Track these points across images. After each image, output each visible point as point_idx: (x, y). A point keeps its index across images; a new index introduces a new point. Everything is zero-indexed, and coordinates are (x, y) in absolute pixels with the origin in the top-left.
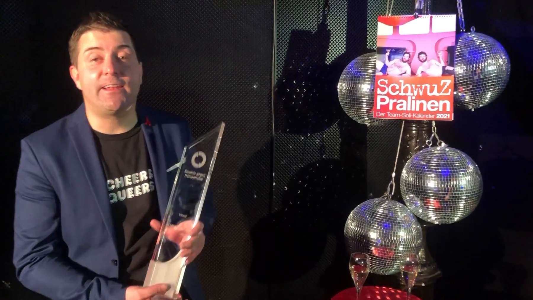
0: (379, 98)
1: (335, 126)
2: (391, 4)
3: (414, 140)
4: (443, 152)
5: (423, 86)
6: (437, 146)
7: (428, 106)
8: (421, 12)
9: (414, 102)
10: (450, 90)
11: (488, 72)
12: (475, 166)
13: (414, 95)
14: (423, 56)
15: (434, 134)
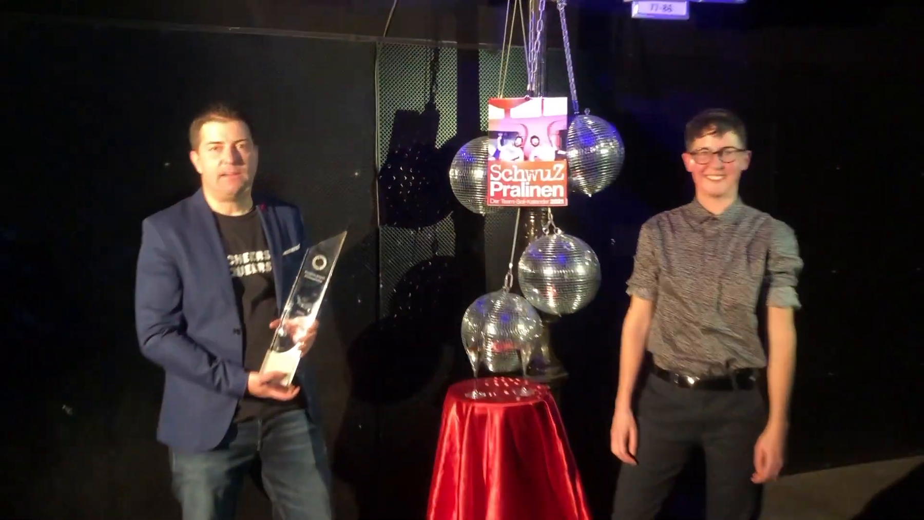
0: (492, 184)
1: (448, 218)
4: (559, 238)
5: (537, 171)
7: (541, 191)
8: (532, 94)
14: (535, 141)
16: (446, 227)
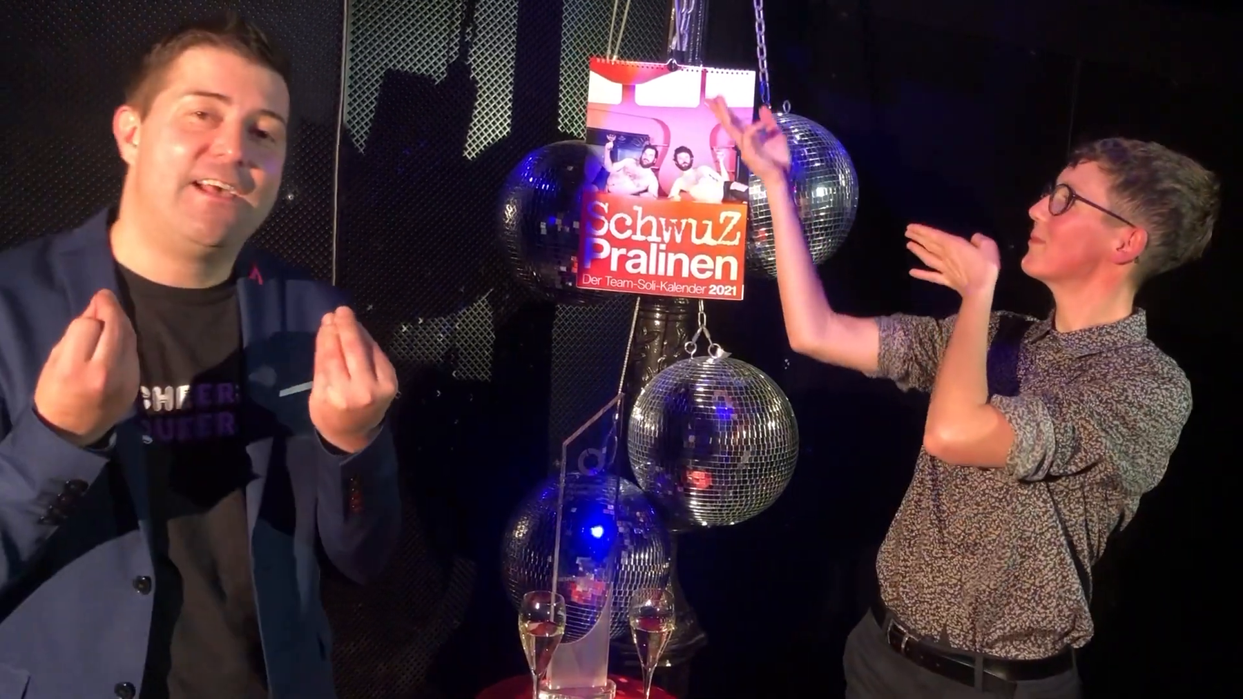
1: (482, 302)
2: (617, 32)
3: (656, 342)
4: (720, 365)
5: (684, 222)
6: (707, 354)
7: (691, 266)
8: (683, 58)
9: (662, 255)
10: (739, 234)
11: (816, 199)
12: (784, 399)
13: (663, 242)
14: (683, 157)
15: (702, 328)
16: (476, 321)
